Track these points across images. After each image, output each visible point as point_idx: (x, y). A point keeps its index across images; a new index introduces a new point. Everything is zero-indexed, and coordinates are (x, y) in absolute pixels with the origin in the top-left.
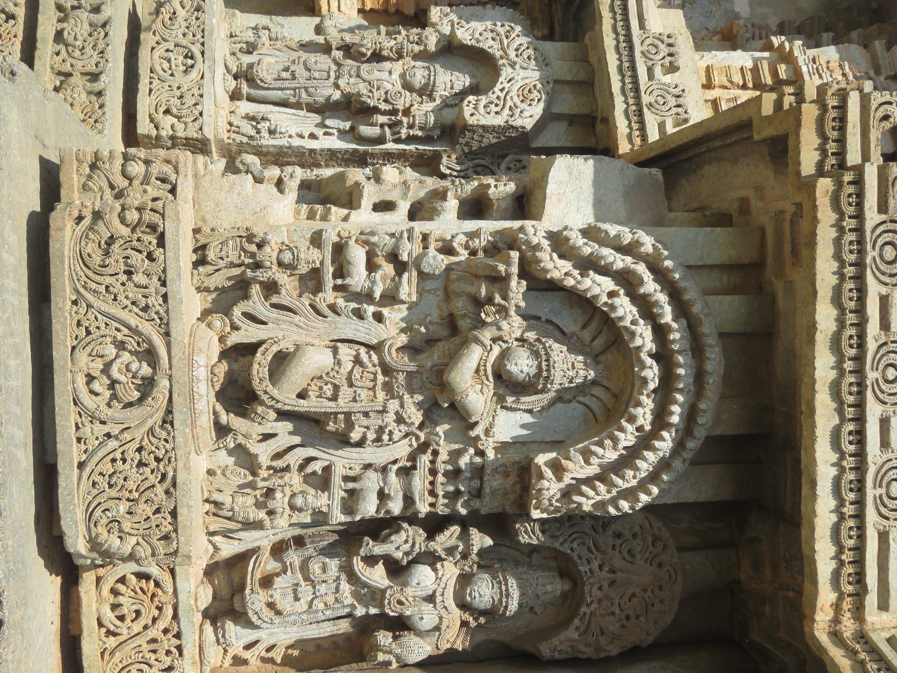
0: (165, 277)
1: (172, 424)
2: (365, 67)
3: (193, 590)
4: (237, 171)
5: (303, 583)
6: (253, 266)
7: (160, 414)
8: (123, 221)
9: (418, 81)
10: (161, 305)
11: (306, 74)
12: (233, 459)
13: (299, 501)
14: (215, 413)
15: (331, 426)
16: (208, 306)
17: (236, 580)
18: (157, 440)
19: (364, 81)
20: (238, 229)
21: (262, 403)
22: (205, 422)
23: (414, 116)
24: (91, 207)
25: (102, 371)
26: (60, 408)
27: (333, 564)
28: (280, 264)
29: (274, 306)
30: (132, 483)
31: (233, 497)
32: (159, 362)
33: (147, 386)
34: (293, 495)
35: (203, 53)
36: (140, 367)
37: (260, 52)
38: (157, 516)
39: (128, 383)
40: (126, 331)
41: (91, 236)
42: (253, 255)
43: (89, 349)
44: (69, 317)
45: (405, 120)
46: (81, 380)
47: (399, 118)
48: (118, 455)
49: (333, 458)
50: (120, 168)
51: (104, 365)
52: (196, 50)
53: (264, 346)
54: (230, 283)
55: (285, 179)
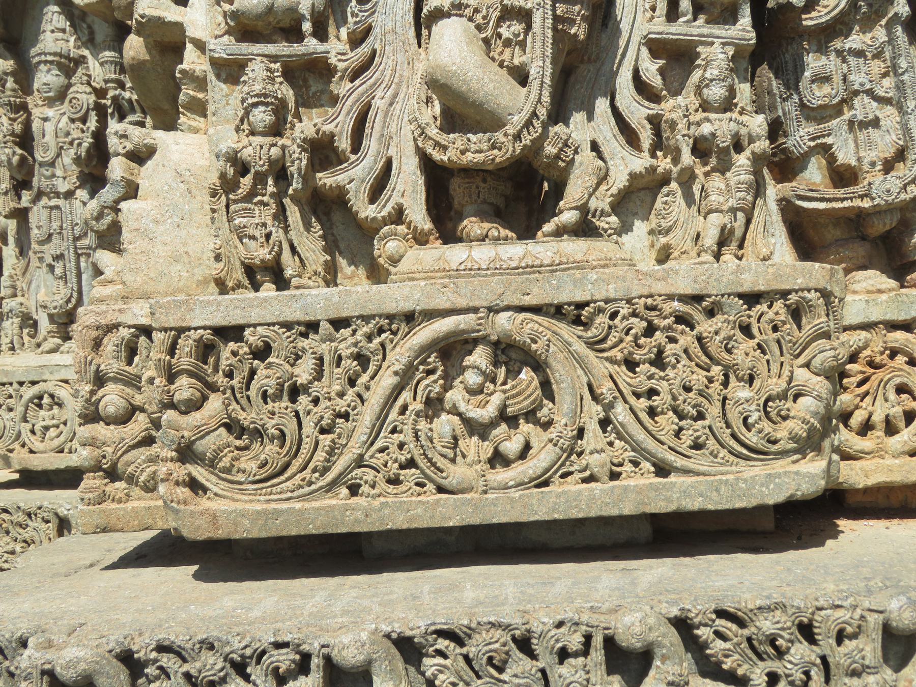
0: (299, 323)
1: (581, 306)
2: (38, 156)
3: (864, 297)
4: (116, 228)
5: (847, 115)
6: (282, 183)
7: (565, 330)
8: (194, 405)
9: (55, 78)
10: (354, 332)
11: (56, 240)
12: (638, 223)
13: (716, 92)
14: (559, 233)
15: (579, 30)
16: (362, 272)
17: (832, 233)
18: (613, 333)
19: (59, 155)
20: (214, 211)
21: (537, 145)
22: (575, 248)
23: (106, 81)
24: (170, 465)
25: (484, 437)
26: (555, 510)
27: (814, 63)
28: (276, 130)
29: (356, 149)
30: (695, 376)
31: (710, 212)
32: (464, 332)
33: (511, 355)
34: (705, 106)
35: (34, 383)
36: (474, 367)
37: (34, 310)
38: (755, 331)
39: (504, 392)
40: (406, 396)
41: (225, 462)
42: (260, 179)
43: (441, 462)
44: (382, 499)
45: (111, 93)
46: (501, 475)
47: (109, 103)
48: (643, 403)
49: (636, 39)
50: (112, 427)
51: (471, 435)
52: (29, 392)
53: (429, 150)
54: (317, 226)
55: (129, 146)
